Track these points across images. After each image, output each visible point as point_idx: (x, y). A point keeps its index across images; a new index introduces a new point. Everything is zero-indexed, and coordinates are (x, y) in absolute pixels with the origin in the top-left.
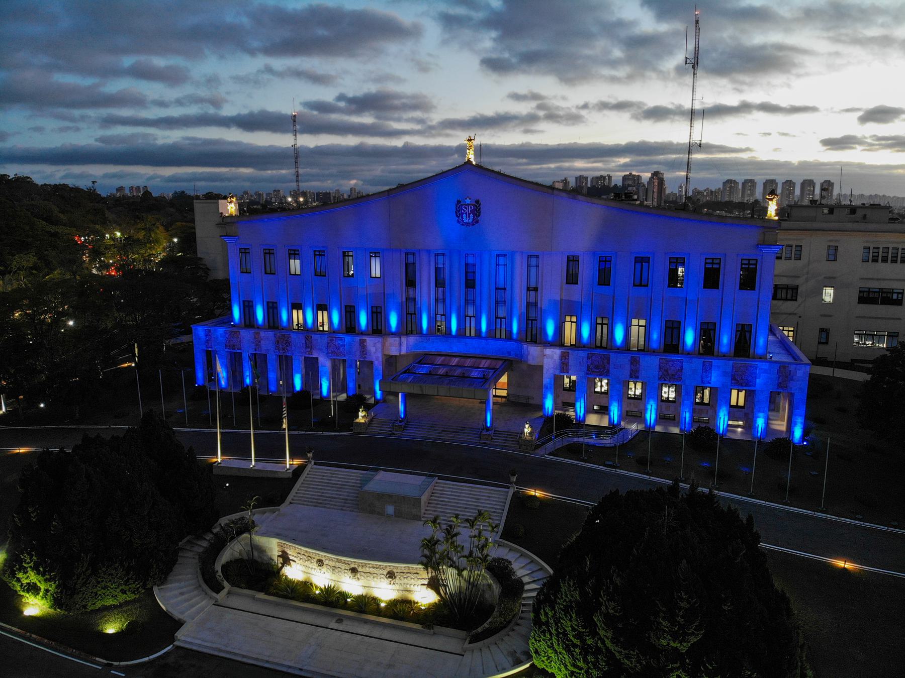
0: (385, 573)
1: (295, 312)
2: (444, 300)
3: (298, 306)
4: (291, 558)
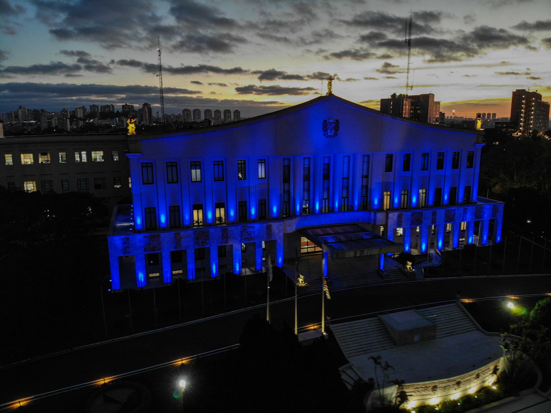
1: (195, 212)
3: (198, 207)
4: (408, 394)
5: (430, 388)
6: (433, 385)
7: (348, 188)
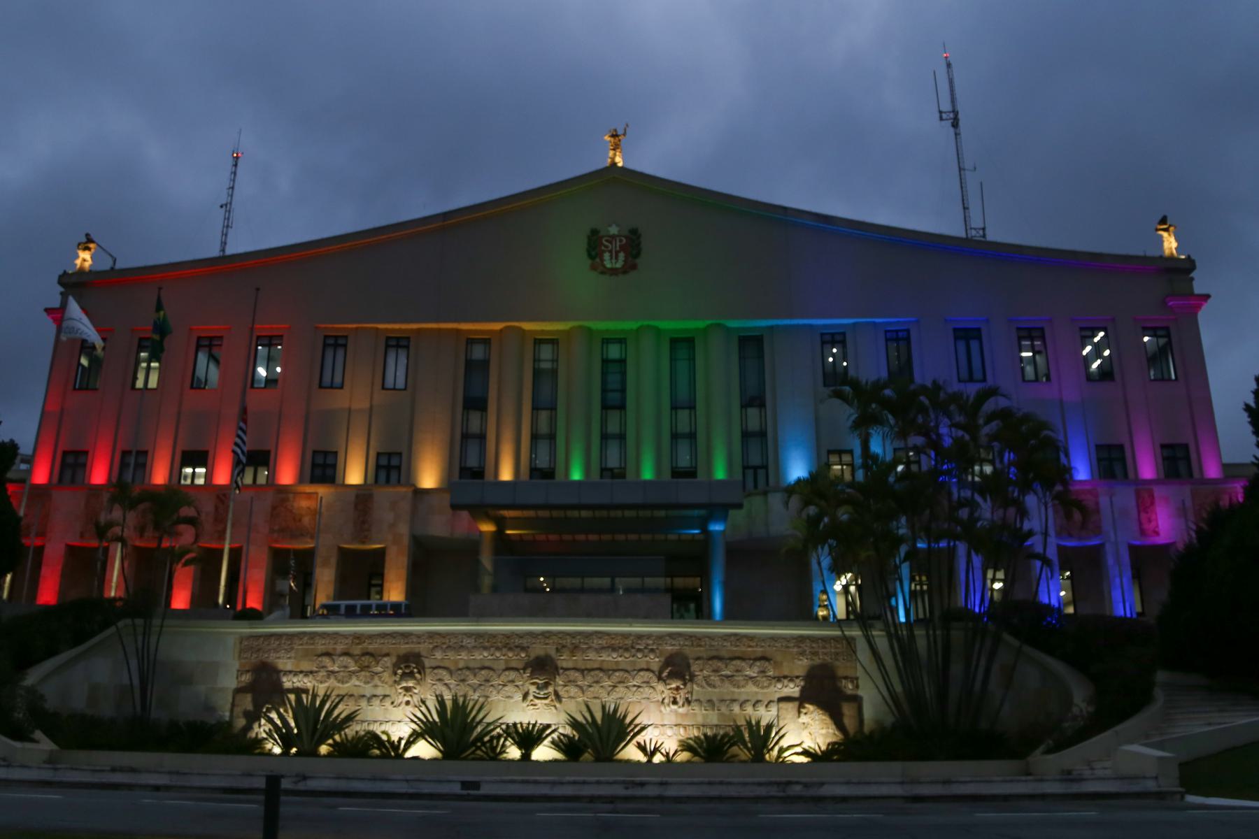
0: (655, 661)
2: (552, 437)
5: (388, 661)
6: (404, 648)
7: (692, 436)
